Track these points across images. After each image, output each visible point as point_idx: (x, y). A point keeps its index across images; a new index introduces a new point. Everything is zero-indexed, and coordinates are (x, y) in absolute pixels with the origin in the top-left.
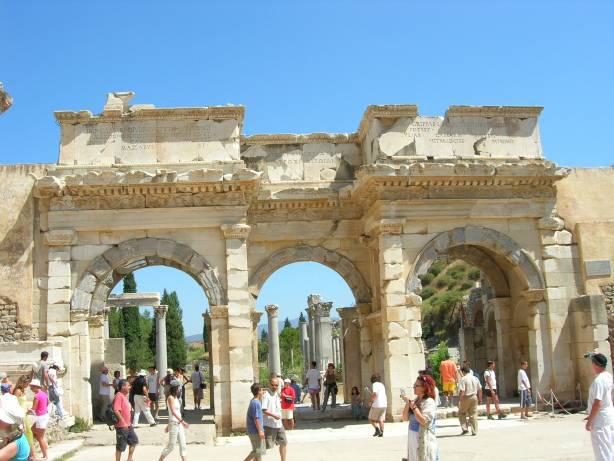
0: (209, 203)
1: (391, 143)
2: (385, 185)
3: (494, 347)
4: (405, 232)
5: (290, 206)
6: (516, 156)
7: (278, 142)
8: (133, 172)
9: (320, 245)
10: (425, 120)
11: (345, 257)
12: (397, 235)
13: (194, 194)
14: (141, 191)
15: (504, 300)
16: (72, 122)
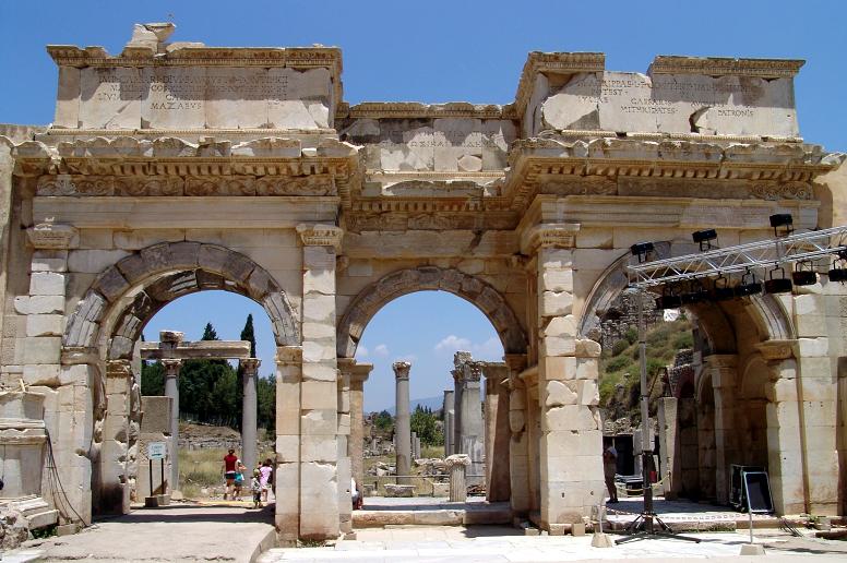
0: (281, 191)
1: (562, 111)
2: (550, 172)
3: (710, 428)
4: (578, 245)
5: (411, 207)
6: (756, 136)
7: (399, 115)
8: (162, 139)
9: (451, 268)
10: (616, 78)
11: (491, 286)
12: (567, 248)
13: (258, 177)
14: (177, 170)
15: (729, 357)
16: (81, 67)
